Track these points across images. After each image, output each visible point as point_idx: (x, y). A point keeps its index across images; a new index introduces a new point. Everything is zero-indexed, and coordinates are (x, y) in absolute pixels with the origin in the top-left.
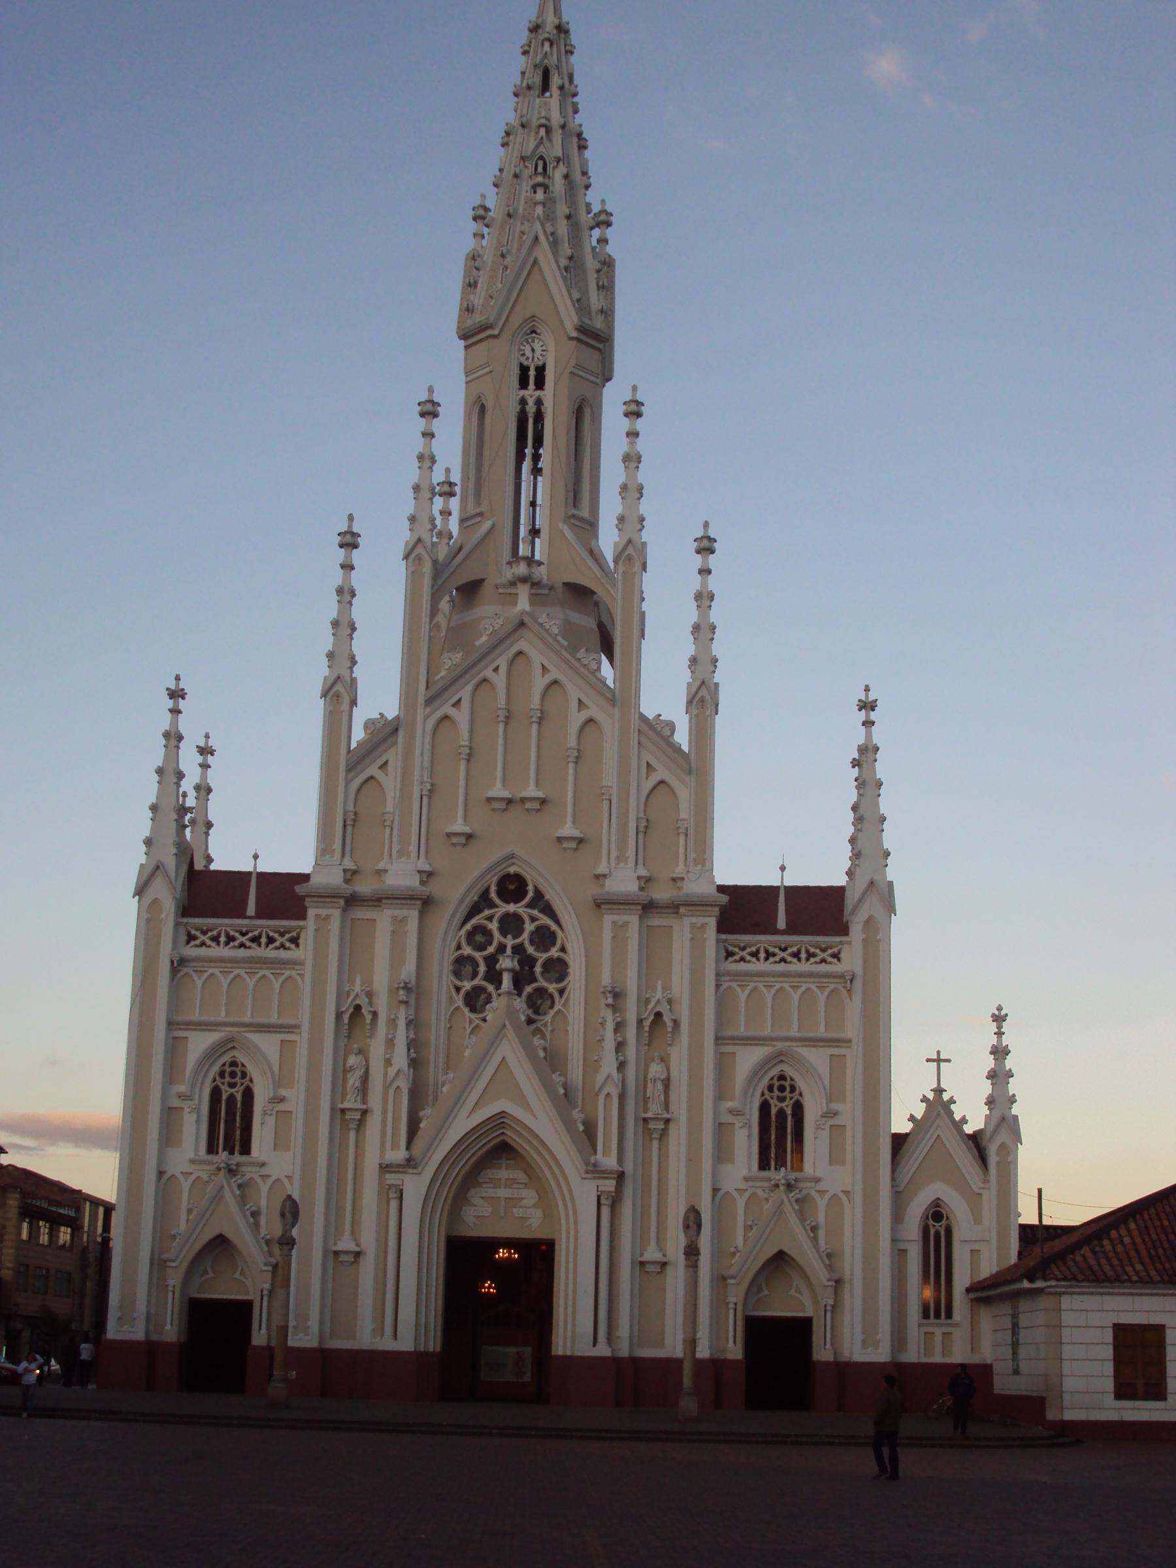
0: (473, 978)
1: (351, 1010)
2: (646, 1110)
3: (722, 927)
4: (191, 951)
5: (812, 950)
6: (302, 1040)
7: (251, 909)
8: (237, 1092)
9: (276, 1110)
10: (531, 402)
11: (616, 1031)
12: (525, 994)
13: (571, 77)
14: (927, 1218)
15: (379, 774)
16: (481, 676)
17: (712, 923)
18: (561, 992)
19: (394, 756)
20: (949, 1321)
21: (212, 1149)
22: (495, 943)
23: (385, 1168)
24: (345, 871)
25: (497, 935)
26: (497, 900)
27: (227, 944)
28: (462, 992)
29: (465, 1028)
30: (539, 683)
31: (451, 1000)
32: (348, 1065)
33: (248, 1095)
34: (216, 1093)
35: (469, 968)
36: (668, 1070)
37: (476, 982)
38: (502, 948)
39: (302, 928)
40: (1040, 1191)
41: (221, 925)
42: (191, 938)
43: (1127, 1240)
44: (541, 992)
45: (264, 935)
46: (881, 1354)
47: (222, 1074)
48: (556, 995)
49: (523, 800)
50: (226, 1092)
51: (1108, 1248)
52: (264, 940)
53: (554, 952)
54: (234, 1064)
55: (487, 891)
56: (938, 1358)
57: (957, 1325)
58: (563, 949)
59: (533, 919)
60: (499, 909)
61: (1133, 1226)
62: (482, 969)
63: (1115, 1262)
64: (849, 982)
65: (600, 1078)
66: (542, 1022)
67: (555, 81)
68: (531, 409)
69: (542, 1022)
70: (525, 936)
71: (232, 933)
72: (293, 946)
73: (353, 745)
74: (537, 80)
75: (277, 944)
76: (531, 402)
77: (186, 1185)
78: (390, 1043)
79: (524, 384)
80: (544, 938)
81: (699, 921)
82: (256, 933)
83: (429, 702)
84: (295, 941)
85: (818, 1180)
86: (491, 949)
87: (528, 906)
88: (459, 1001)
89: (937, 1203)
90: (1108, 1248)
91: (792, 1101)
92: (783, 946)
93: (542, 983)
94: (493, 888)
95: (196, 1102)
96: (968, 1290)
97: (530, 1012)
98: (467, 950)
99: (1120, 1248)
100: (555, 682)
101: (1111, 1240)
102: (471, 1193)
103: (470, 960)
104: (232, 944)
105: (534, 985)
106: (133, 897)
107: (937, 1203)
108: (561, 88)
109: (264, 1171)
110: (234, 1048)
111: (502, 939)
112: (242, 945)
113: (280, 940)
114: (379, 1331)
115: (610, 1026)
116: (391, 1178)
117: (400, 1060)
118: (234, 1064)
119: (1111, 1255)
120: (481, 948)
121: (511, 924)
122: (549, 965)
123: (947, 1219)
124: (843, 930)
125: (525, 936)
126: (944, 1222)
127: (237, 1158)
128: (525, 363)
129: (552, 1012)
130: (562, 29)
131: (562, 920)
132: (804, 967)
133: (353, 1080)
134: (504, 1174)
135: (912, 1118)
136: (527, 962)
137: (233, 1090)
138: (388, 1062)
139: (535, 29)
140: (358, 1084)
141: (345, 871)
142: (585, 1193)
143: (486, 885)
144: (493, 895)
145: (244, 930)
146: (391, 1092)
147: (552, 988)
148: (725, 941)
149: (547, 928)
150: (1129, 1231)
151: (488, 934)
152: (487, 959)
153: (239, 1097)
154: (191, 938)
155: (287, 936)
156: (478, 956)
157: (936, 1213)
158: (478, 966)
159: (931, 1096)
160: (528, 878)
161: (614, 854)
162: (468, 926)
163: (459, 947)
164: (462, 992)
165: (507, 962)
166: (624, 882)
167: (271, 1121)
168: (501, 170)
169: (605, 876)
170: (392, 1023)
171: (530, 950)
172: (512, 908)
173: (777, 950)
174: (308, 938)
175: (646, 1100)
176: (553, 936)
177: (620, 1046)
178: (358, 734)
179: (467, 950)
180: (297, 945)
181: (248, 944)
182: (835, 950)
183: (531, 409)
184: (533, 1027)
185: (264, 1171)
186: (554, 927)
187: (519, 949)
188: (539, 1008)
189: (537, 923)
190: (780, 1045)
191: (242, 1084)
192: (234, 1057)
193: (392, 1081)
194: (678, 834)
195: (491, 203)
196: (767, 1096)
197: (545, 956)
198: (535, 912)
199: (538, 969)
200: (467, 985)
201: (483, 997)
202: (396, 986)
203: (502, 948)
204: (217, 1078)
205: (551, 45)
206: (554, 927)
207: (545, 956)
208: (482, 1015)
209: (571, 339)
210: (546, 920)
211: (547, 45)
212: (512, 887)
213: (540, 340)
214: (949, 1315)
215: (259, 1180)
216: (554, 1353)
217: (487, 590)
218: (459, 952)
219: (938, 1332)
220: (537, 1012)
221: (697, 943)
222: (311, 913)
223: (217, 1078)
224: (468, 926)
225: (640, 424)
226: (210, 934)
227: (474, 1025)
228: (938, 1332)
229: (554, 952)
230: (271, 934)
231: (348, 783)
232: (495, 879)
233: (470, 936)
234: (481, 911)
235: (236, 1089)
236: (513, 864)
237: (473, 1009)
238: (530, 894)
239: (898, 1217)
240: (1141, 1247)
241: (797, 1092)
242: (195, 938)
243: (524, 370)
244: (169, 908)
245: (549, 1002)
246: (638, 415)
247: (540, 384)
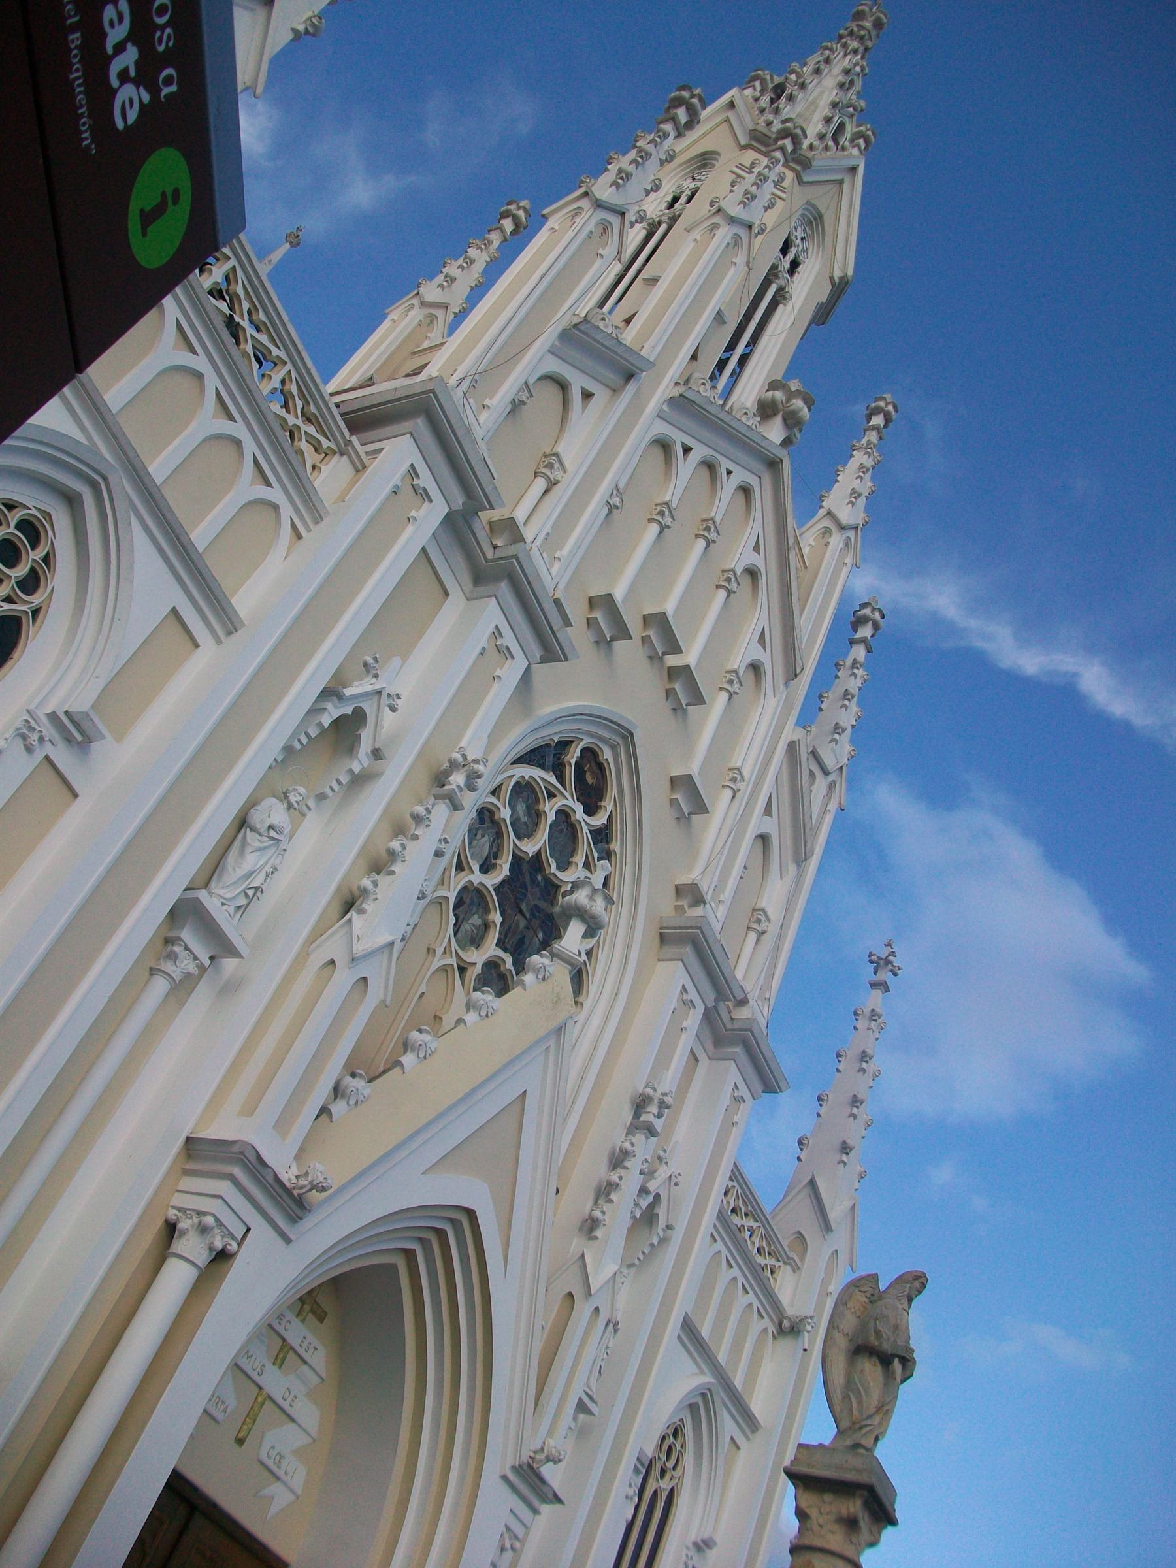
9: (49, 749)
26: (570, 773)
29: (430, 951)
55: (565, 744)
160: (612, 790)
192: (48, 516)
194: (748, 928)
209: (832, 278)
236: (614, 748)
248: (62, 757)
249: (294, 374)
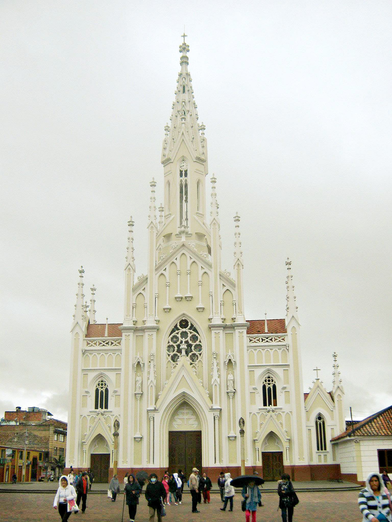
0: (173, 352)
1: (137, 363)
2: (227, 389)
3: (248, 333)
4: (88, 348)
5: (276, 338)
6: (123, 372)
7: (106, 334)
10: (184, 181)
11: (217, 366)
12: (189, 356)
13: (191, 87)
14: (317, 419)
15: (142, 292)
16: (171, 261)
17: (245, 331)
18: (200, 354)
19: (148, 286)
20: (325, 451)
21: (96, 407)
22: (180, 341)
23: (148, 411)
24: (133, 321)
25: (180, 338)
27: (99, 345)
28: (170, 356)
29: (171, 367)
30: (190, 262)
31: (167, 358)
32: (136, 380)
35: (172, 349)
36: (234, 376)
37: (175, 352)
38: (181, 342)
39: (121, 339)
40: (351, 408)
41: (97, 339)
42: (88, 344)
43: (380, 422)
44: (194, 355)
45: (110, 342)
46: (305, 462)
48: (199, 355)
49: (186, 298)
50: (100, 390)
51: (374, 425)
52: (110, 343)
53: (197, 343)
56: (323, 463)
57: (328, 452)
58: (200, 342)
59: (191, 333)
60: (180, 331)
61: (381, 418)
62: (176, 348)
63: (377, 429)
64: (288, 347)
65: (213, 380)
66: (195, 364)
67: (186, 89)
68: (184, 183)
69: (195, 364)
70: (188, 339)
71: (100, 342)
72: (119, 345)
73: (135, 284)
74: (181, 89)
75: (114, 344)
76: (184, 181)
77: (89, 418)
78: (149, 373)
79: (181, 175)
80: (194, 338)
81: (241, 331)
82: (107, 341)
83: (156, 270)
84: (119, 343)
85: (281, 409)
86: (178, 343)
87: (190, 329)
88: (170, 358)
89: (320, 414)
90: (374, 425)
91: (272, 385)
92: (267, 337)
93: (194, 352)
94: (178, 324)
96: (331, 441)
97: (191, 361)
98: (171, 343)
99: (377, 425)
100: (194, 262)
101: (374, 422)
102: (176, 417)
103: (172, 346)
104: (100, 345)
105: (192, 353)
106: (70, 332)
107: (320, 414)
108: (189, 91)
111: (182, 339)
112: (104, 345)
113: (115, 343)
114: (149, 462)
115: (215, 364)
116: (151, 414)
117: (152, 377)
119: (375, 427)
120: (175, 342)
121: (184, 335)
122: (196, 346)
123: (323, 419)
124: (285, 331)
125: (188, 339)
126: (322, 420)
127: (104, 410)
128: (181, 170)
129: (198, 361)
130: (188, 75)
131: (199, 332)
132: (274, 343)
133: (139, 384)
134: (185, 411)
135: (310, 388)
136: (189, 346)
138: (148, 379)
139: (180, 75)
140: (140, 386)
141: (133, 321)
142: (210, 416)
143: (176, 324)
144: (178, 326)
145: (104, 341)
146: (150, 387)
147: (197, 353)
148: (249, 337)
149: (195, 335)
150: (380, 419)
151: (177, 338)
152: (177, 346)
154: (88, 344)
155: (117, 342)
156: (174, 345)
157: (320, 417)
158: (175, 348)
159: (315, 381)
160: (189, 321)
161: (214, 311)
162: (171, 336)
163: (169, 343)
164: (170, 356)
165: (183, 346)
166: (217, 321)
168: (172, 115)
169: (212, 319)
170: (149, 366)
171: (190, 342)
172: (184, 330)
173: (265, 339)
174: (123, 342)
175: (227, 386)
176: (197, 337)
177: (218, 370)
178: (136, 281)
179: (171, 343)
180: (120, 344)
181: (105, 345)
182: (283, 338)
183: (184, 183)
184: (192, 365)
186: (197, 335)
187: (187, 342)
188: (193, 360)
189: (192, 334)
190: (268, 367)
193: (149, 385)
195: (169, 125)
196: (265, 383)
197: (195, 344)
198: (191, 331)
199: (193, 348)
200: (172, 354)
201: (177, 357)
202: (150, 355)
203: (181, 342)
205: (185, 79)
206: (197, 335)
207: (195, 344)
208: (176, 363)
209: (194, 162)
210: (196, 333)
211: (184, 79)
212: (184, 324)
213: (186, 163)
214: (325, 449)
216: (203, 466)
217: (173, 236)
218: (169, 344)
219: (322, 455)
220: (193, 361)
221: (241, 338)
222: (124, 334)
224: (171, 336)
225: (215, 185)
226: (94, 342)
227: (174, 366)
228: (322, 455)
229: (197, 343)
230: (112, 341)
231: (133, 295)
232: (179, 322)
233: (172, 339)
234: (175, 331)
235: (103, 389)
237: (174, 361)
238: (190, 325)
239: (308, 419)
240: (385, 424)
241: (274, 382)
242: (89, 344)
243: (181, 172)
244: (82, 336)
245: (196, 358)
246: (215, 182)
247: (186, 175)
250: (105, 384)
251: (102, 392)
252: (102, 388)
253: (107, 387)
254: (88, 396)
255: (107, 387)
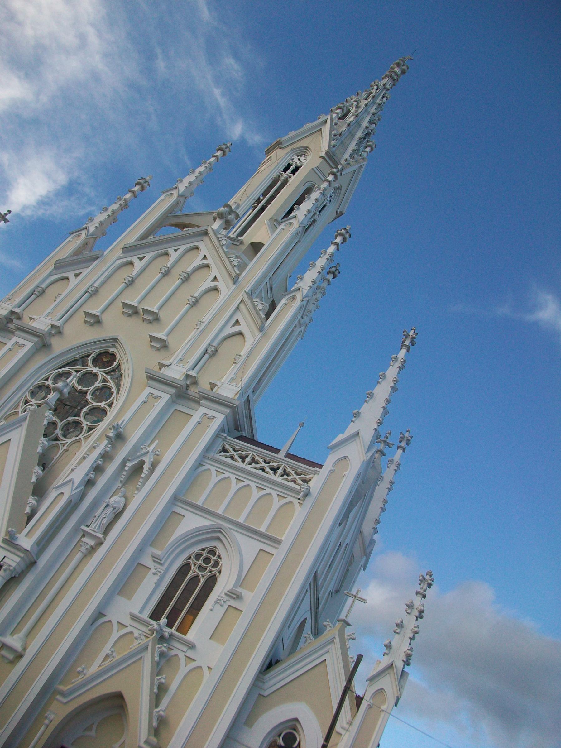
8: (203, 576)
9: (228, 603)
33: (211, 582)
34: (185, 569)
47: (198, 556)
50: (194, 570)
54: (212, 552)
95: (164, 568)
109: (190, 653)
110: (219, 539)
118: (212, 552)
137: (200, 573)
153: (202, 581)
167: (220, 611)
185: (190, 653)
191: (211, 572)
204: (192, 558)
215: (183, 660)
223: (192, 558)
235: (203, 573)
248: (232, 603)
249: (255, 454)
250: (216, 564)
251: (196, 579)
252: (200, 568)
253: (218, 574)
254: (153, 571)
255: (218, 574)
